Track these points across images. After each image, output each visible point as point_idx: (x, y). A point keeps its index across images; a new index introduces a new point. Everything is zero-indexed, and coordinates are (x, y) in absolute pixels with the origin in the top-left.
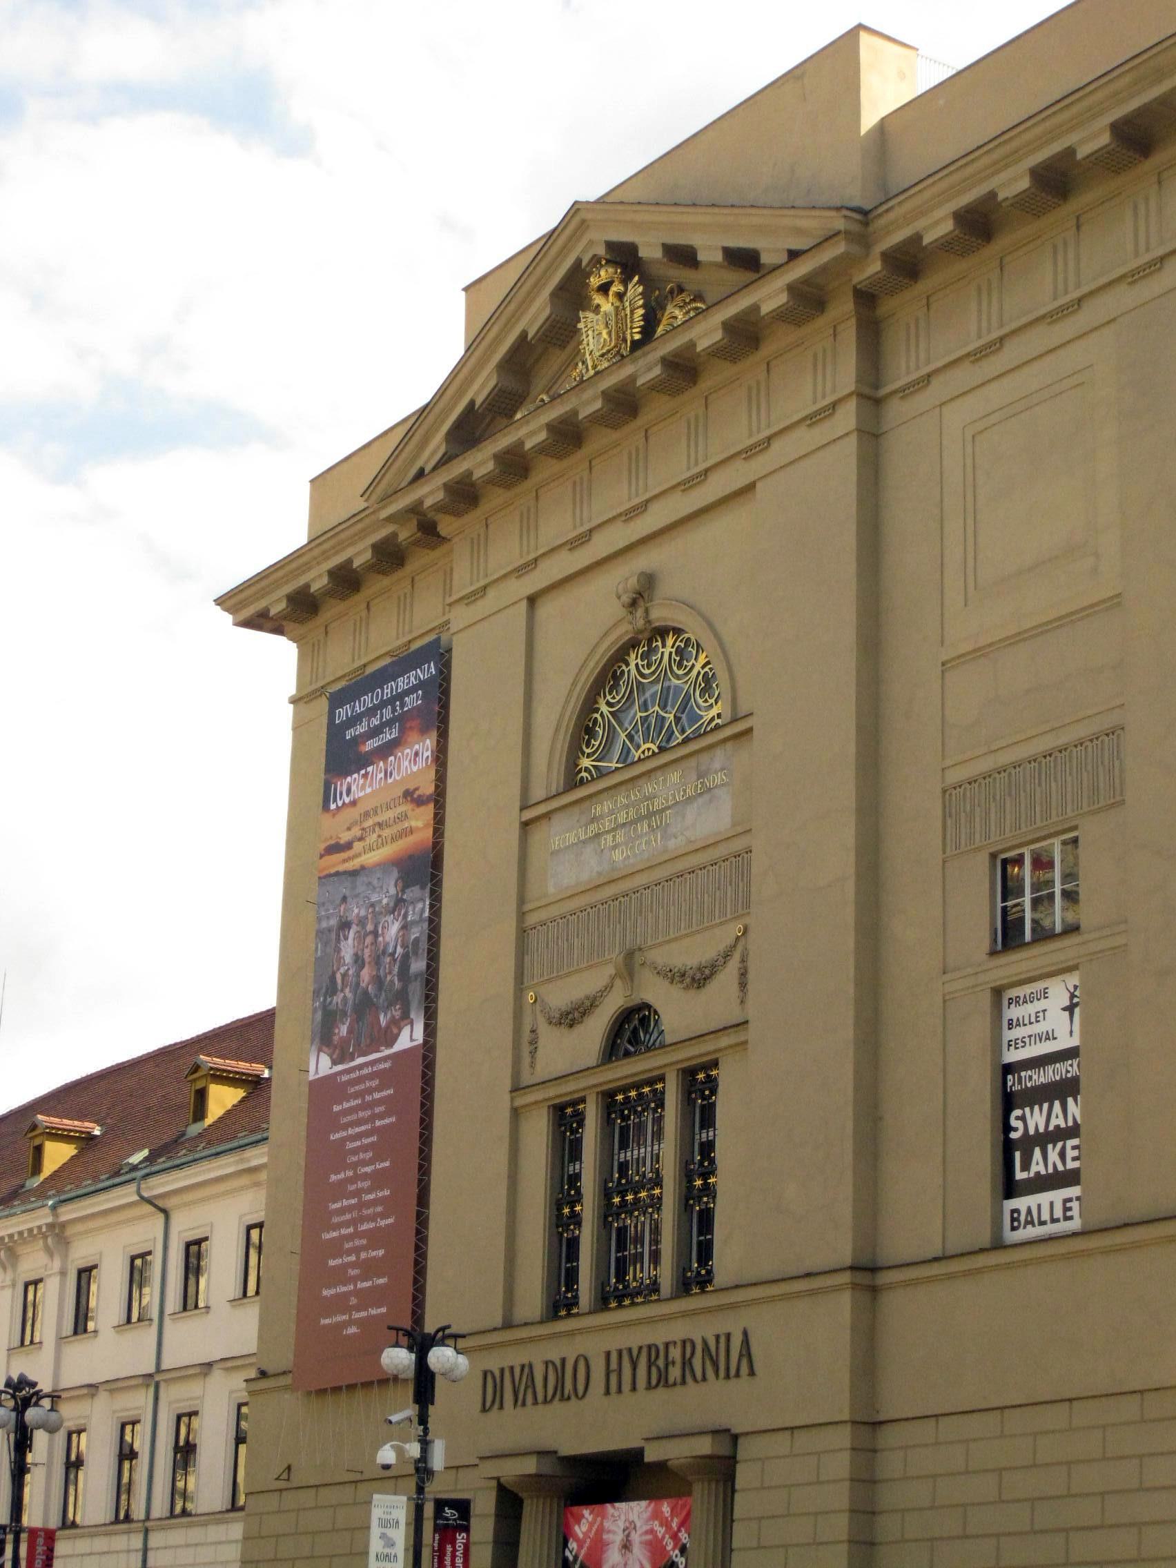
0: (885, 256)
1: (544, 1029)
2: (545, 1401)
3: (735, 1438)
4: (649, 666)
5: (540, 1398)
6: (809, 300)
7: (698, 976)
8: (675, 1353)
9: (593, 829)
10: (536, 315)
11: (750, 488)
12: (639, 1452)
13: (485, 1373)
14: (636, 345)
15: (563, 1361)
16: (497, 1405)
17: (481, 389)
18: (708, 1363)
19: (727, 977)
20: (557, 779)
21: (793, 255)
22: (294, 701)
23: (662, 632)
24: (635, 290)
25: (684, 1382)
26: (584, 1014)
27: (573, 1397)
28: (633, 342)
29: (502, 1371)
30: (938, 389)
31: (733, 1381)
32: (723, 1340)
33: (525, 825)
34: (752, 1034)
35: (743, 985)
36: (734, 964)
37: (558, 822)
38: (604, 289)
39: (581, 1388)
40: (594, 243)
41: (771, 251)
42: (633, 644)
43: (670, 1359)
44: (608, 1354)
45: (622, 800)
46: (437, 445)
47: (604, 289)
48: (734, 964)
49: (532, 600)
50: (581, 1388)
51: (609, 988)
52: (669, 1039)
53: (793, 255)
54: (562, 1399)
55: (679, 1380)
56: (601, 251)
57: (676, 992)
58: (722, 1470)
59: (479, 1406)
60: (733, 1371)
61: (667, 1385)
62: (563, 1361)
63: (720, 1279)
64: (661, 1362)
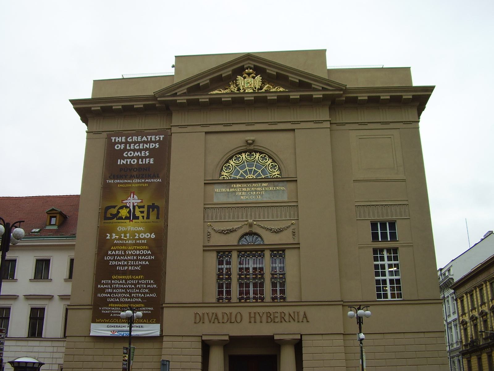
0: (346, 97)
1: (212, 233)
2: (223, 323)
4: (250, 158)
5: (221, 321)
6: (325, 97)
7: (278, 230)
8: (278, 315)
9: (231, 190)
10: (226, 73)
11: (293, 130)
12: (273, 336)
13: (196, 314)
14: (258, 89)
15: (231, 313)
16: (202, 321)
17: (203, 82)
18: (290, 317)
19: (289, 233)
21: (324, 89)
22: (87, 132)
23: (256, 152)
24: (259, 78)
25: (281, 322)
26: (231, 232)
27: (235, 322)
28: (258, 88)
29: (203, 314)
30: (347, 127)
32: (296, 314)
33: (205, 183)
34: (301, 246)
35: (294, 235)
36: (290, 230)
37: (216, 186)
38: (249, 74)
39: (239, 320)
40: (252, 64)
41: (315, 85)
42: (245, 152)
44: (250, 313)
45: (245, 185)
46: (184, 90)
47: (249, 74)
48: (290, 230)
49: (207, 133)
50: (239, 320)
51: (241, 227)
52: (266, 243)
53: (324, 89)
54: (231, 322)
55: (279, 321)
56: (253, 66)
57: (268, 233)
59: (194, 322)
60: (301, 320)
61: (274, 322)
62: (231, 313)
63: (288, 299)
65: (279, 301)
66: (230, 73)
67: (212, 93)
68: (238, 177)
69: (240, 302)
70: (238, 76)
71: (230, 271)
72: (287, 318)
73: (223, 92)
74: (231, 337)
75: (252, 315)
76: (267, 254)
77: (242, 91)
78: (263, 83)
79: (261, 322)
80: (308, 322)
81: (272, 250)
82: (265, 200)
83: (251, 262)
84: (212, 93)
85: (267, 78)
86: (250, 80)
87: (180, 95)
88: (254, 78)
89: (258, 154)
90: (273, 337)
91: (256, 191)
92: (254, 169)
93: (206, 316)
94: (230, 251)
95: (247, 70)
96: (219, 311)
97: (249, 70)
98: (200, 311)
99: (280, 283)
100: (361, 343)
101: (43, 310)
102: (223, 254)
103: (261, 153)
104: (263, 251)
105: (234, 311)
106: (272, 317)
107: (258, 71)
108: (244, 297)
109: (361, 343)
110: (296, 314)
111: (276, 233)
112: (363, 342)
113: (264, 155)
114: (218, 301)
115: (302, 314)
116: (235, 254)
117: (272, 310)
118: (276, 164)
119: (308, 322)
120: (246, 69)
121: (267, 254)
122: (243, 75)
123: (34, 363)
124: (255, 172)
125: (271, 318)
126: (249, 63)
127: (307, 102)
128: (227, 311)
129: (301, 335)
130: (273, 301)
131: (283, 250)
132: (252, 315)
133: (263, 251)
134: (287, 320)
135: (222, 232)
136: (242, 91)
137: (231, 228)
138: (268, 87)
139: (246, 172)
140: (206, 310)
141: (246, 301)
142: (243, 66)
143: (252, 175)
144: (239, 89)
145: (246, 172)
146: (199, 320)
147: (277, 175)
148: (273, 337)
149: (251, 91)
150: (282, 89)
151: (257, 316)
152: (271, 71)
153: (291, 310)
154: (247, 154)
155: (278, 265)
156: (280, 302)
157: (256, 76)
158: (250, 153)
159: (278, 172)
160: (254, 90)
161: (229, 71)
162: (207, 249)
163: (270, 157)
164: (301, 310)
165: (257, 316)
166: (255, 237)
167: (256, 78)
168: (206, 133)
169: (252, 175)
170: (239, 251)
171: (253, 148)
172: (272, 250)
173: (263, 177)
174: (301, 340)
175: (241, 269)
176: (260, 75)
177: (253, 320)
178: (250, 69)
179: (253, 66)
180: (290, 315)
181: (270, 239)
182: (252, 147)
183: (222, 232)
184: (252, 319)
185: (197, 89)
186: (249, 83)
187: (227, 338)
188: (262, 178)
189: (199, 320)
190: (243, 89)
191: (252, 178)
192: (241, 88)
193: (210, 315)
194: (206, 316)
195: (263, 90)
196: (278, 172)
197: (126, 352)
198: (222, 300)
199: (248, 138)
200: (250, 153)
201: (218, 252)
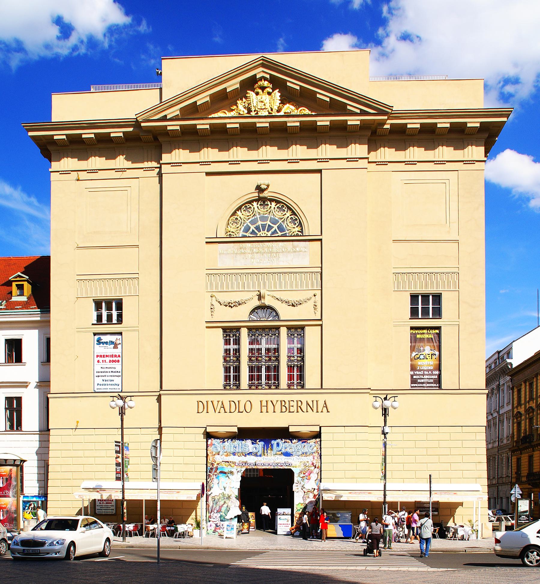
2: (230, 412)
3: (320, 428)
5: (227, 410)
8: (295, 404)
10: (233, 85)
11: (320, 171)
20: (222, 233)
23: (271, 200)
24: (277, 94)
26: (240, 304)
31: (320, 413)
32: (315, 403)
33: (206, 242)
35: (315, 309)
36: (311, 304)
38: (263, 88)
42: (257, 201)
43: (291, 404)
47: (263, 88)
48: (311, 304)
55: (296, 411)
57: (284, 305)
58: (318, 435)
60: (320, 410)
64: (287, 405)
65: (295, 387)
66: (238, 86)
67: (213, 116)
68: (247, 234)
69: (250, 388)
70: (248, 91)
71: (239, 352)
72: (304, 407)
73: (229, 114)
74: (239, 429)
75: (264, 403)
76: (284, 331)
77: (253, 114)
78: (283, 101)
79: (274, 412)
80: (328, 412)
81: (289, 328)
82: (282, 265)
83: (264, 341)
84: (213, 116)
85: (288, 96)
86: (265, 97)
87: (171, 120)
88: (269, 94)
89: (274, 204)
90: (287, 428)
91: (271, 253)
92: (269, 225)
93: (210, 404)
94: (238, 329)
95: (260, 83)
96: (226, 399)
97: (263, 81)
98: (204, 399)
99: (298, 367)
100: (385, 437)
101: (19, 399)
102: (231, 333)
103: (277, 202)
104: (278, 328)
105: (243, 399)
106: (287, 405)
107: (277, 83)
108: (255, 381)
109: (385, 437)
110: (315, 403)
111: (293, 305)
112: (387, 436)
113: (282, 204)
114: (225, 388)
115: (321, 404)
116: (244, 332)
117: (287, 398)
118: (297, 217)
119: (328, 412)
120: (259, 81)
121: (284, 331)
122: (255, 89)
123: (15, 460)
124: (270, 227)
125: (285, 407)
126: (263, 71)
127: (341, 135)
128: (236, 398)
129: (320, 428)
130: (289, 388)
131: (302, 328)
132: (264, 403)
133: (278, 328)
134: (305, 410)
135: (229, 305)
136: (253, 114)
137: (239, 300)
138: (289, 108)
139: (257, 228)
140: (210, 398)
141: (257, 387)
142: (255, 75)
143: (266, 232)
144: (249, 111)
145: (257, 228)
146: (203, 408)
147: (297, 232)
148: (287, 428)
149: (266, 114)
150: (307, 112)
151: (270, 404)
152: (294, 84)
153: (309, 398)
154: (259, 203)
155: (296, 345)
156: (297, 389)
157: (273, 91)
158: (264, 202)
159: (299, 229)
160: (269, 113)
161: (236, 84)
162: (211, 325)
163: (289, 208)
164: (322, 399)
165: (270, 404)
166: (268, 310)
167: (273, 94)
168: (208, 174)
169: (266, 232)
170: (250, 329)
171: (266, 196)
172: (289, 328)
173: (280, 234)
174: (320, 432)
175: (251, 350)
176: (278, 90)
177: (264, 409)
178: (265, 80)
179: (268, 76)
180: (308, 404)
181: (287, 313)
182: (265, 194)
183: (229, 305)
184: (264, 407)
185: (192, 111)
186: (262, 102)
187: (235, 430)
188: (279, 236)
189: (203, 408)
190: (255, 111)
191: (265, 235)
192: (253, 109)
193: (215, 404)
194: (210, 404)
195: (282, 113)
196: (299, 229)
197: (118, 450)
198: (230, 386)
199: (262, 182)
200: (264, 202)
201: (225, 329)
